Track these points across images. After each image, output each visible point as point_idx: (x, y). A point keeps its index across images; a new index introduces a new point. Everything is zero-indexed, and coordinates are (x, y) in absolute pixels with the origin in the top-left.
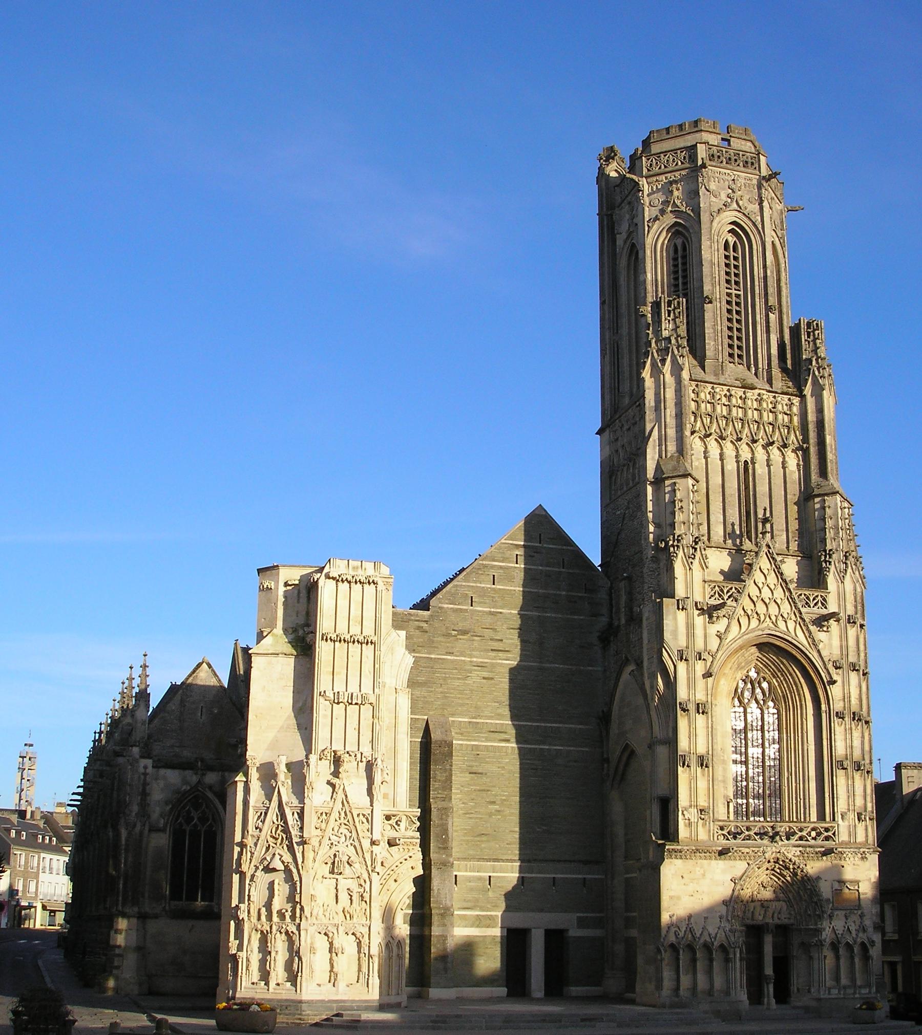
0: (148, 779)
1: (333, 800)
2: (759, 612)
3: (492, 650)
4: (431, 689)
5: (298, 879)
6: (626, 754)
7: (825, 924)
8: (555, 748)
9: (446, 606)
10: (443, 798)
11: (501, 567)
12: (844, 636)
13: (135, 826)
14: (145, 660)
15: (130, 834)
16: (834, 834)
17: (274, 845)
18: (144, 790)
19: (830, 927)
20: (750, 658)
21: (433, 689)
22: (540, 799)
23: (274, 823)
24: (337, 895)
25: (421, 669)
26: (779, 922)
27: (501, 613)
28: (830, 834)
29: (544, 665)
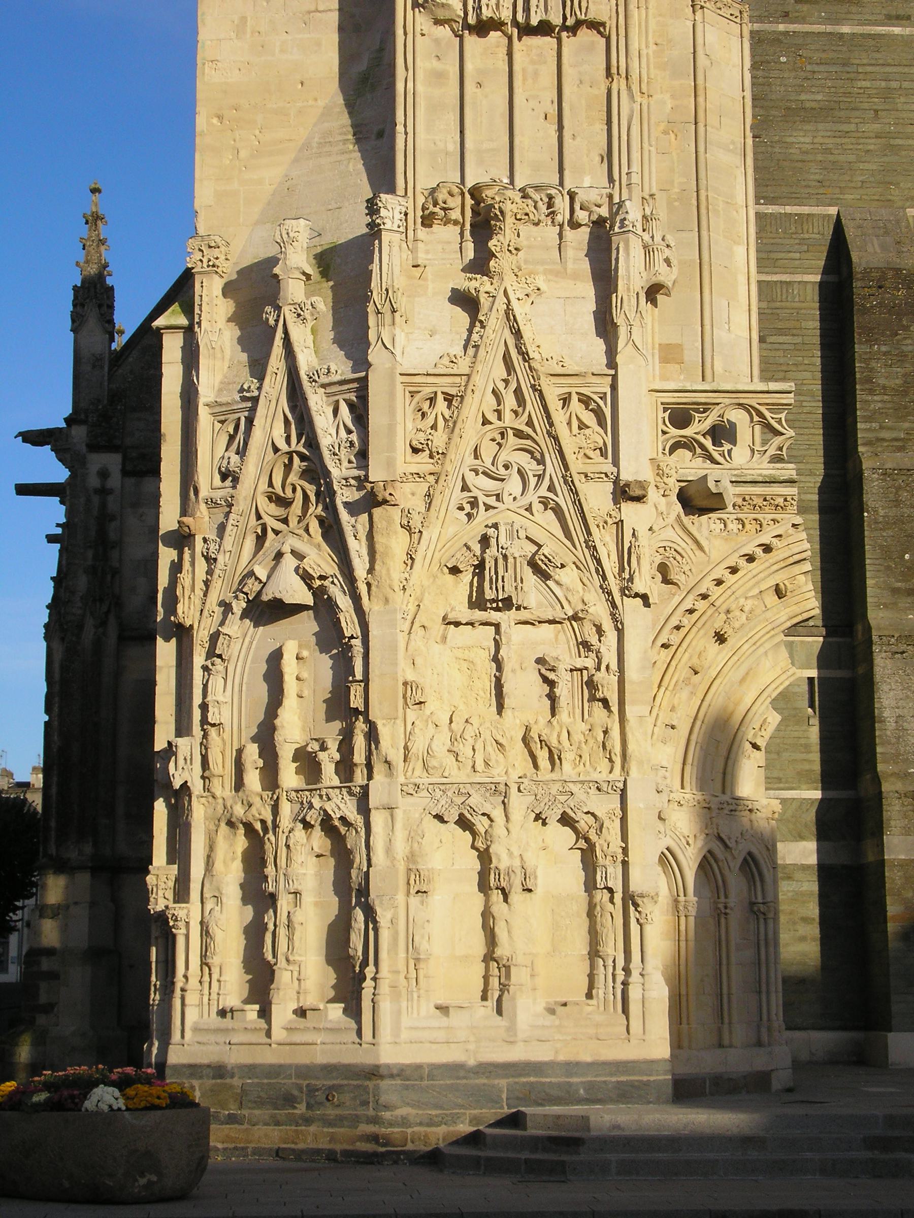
0: (113, 504)
1: (471, 351)
4: (845, 127)
5: (358, 632)
10: (896, 440)
13: (80, 627)
17: (279, 526)
21: (852, 127)
23: (276, 450)
24: (498, 680)
25: (809, 68)
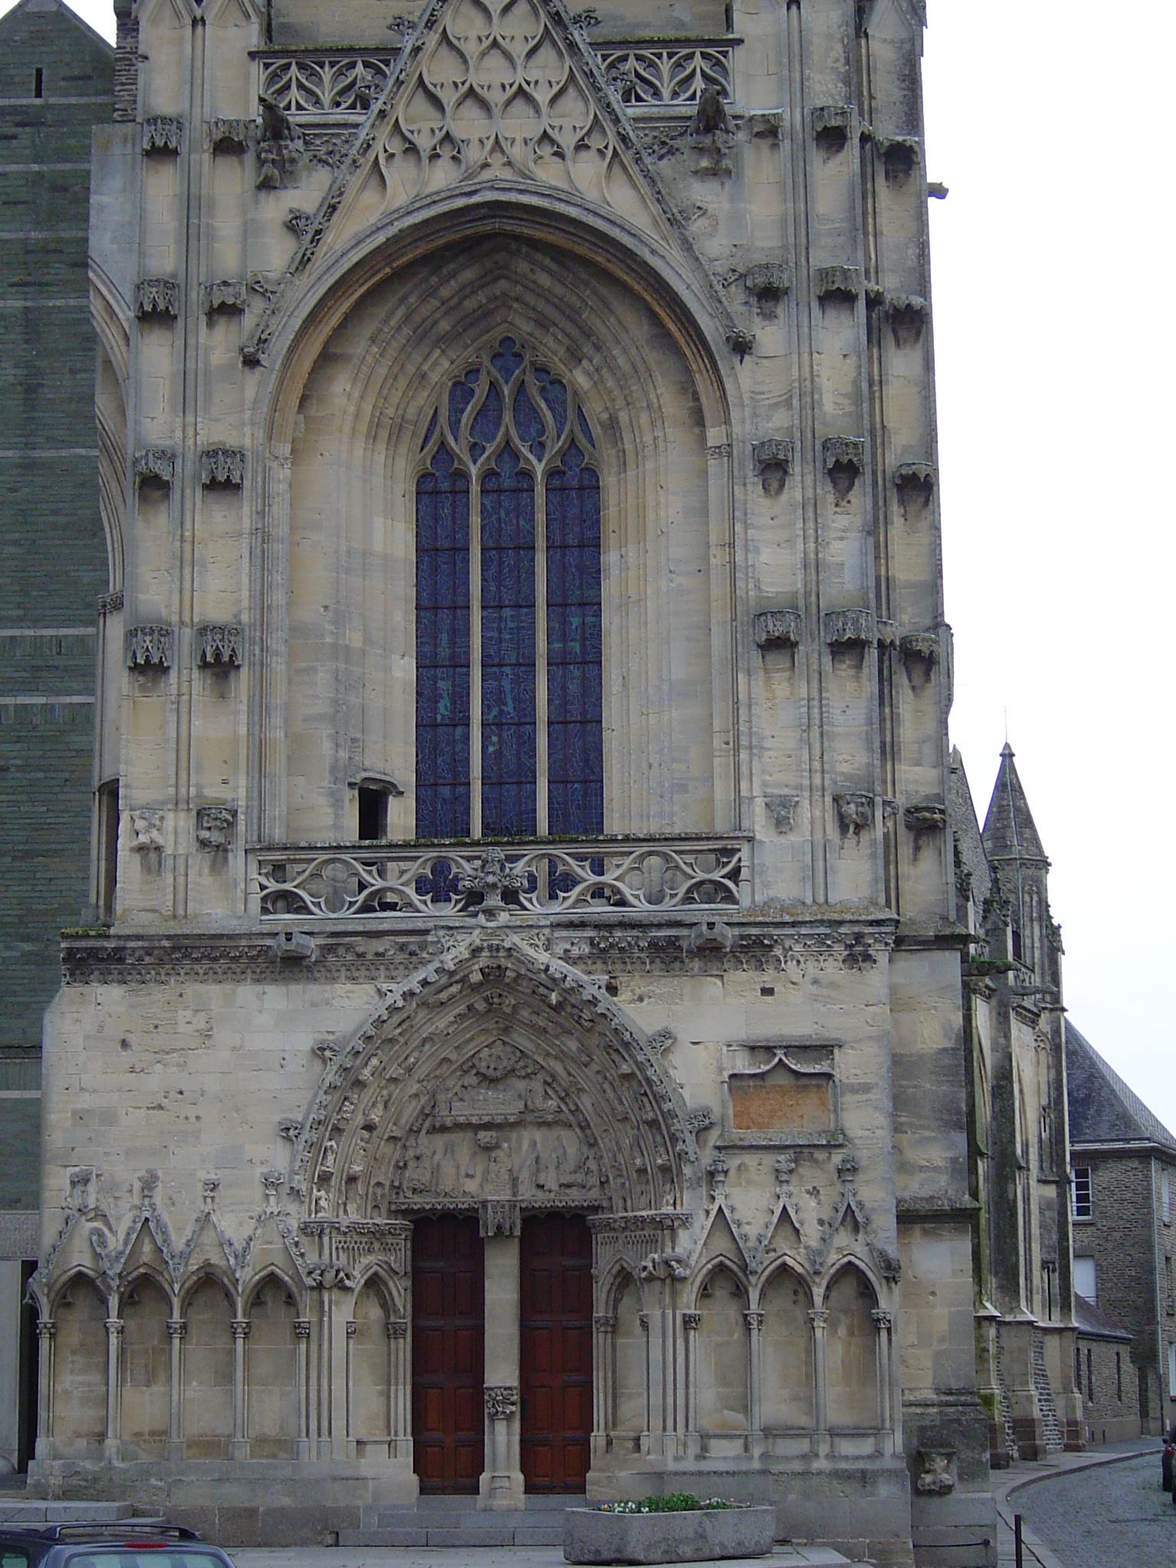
2: (458, 133)
7: (691, 1201)
8: (68, 700)
12: (800, 186)
16: (735, 875)
19: (708, 1212)
20: (470, 304)
22: (14, 858)
26: (541, 1200)
29: (37, 454)
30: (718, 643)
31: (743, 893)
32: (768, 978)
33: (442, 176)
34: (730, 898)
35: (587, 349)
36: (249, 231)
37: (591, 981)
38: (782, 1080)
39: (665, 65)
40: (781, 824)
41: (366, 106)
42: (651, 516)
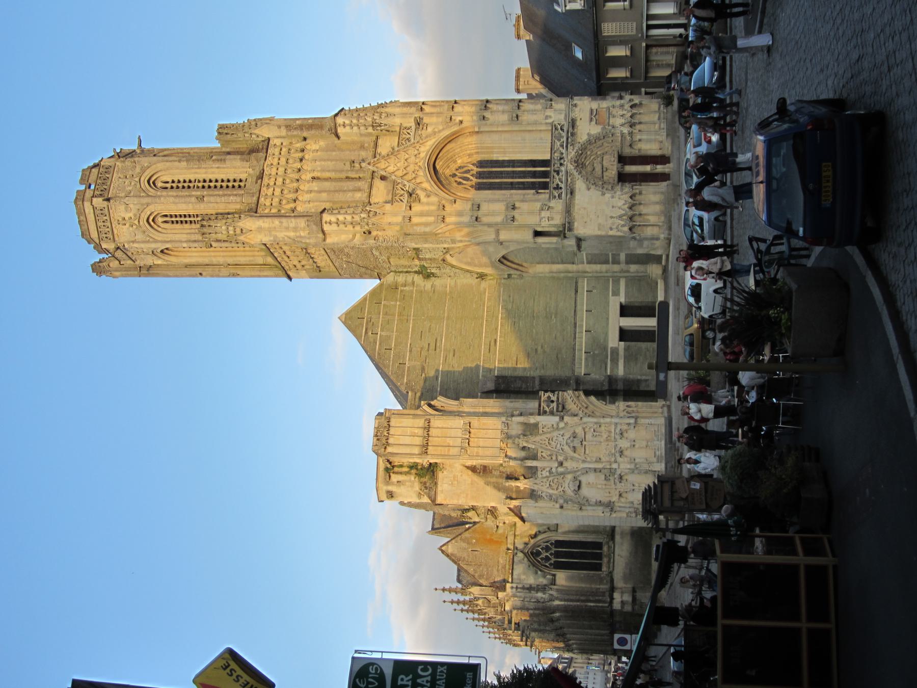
0: (520, 586)
3: (435, 350)
6: (505, 262)
9: (405, 381)
11: (380, 344)
14: (440, 589)
15: (557, 599)
18: (528, 589)
27: (410, 344)
28: (559, 127)
30: (516, 128)
31: (562, 123)
32: (578, 119)
33: (421, 173)
34: (563, 125)
35: (454, 158)
36: (428, 204)
37: (577, 146)
38: (597, 116)
39: (404, 136)
40: (550, 117)
41: (405, 185)
42: (489, 145)
